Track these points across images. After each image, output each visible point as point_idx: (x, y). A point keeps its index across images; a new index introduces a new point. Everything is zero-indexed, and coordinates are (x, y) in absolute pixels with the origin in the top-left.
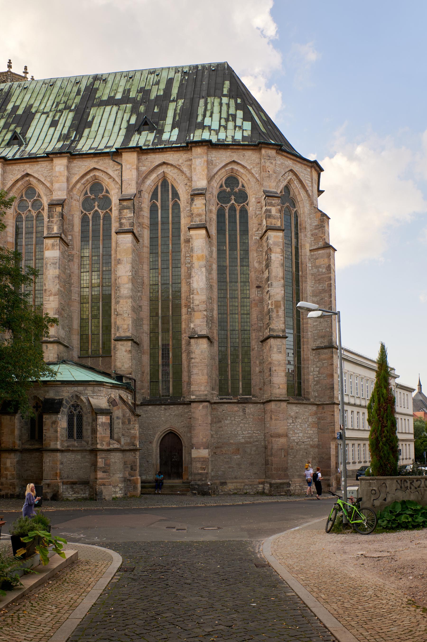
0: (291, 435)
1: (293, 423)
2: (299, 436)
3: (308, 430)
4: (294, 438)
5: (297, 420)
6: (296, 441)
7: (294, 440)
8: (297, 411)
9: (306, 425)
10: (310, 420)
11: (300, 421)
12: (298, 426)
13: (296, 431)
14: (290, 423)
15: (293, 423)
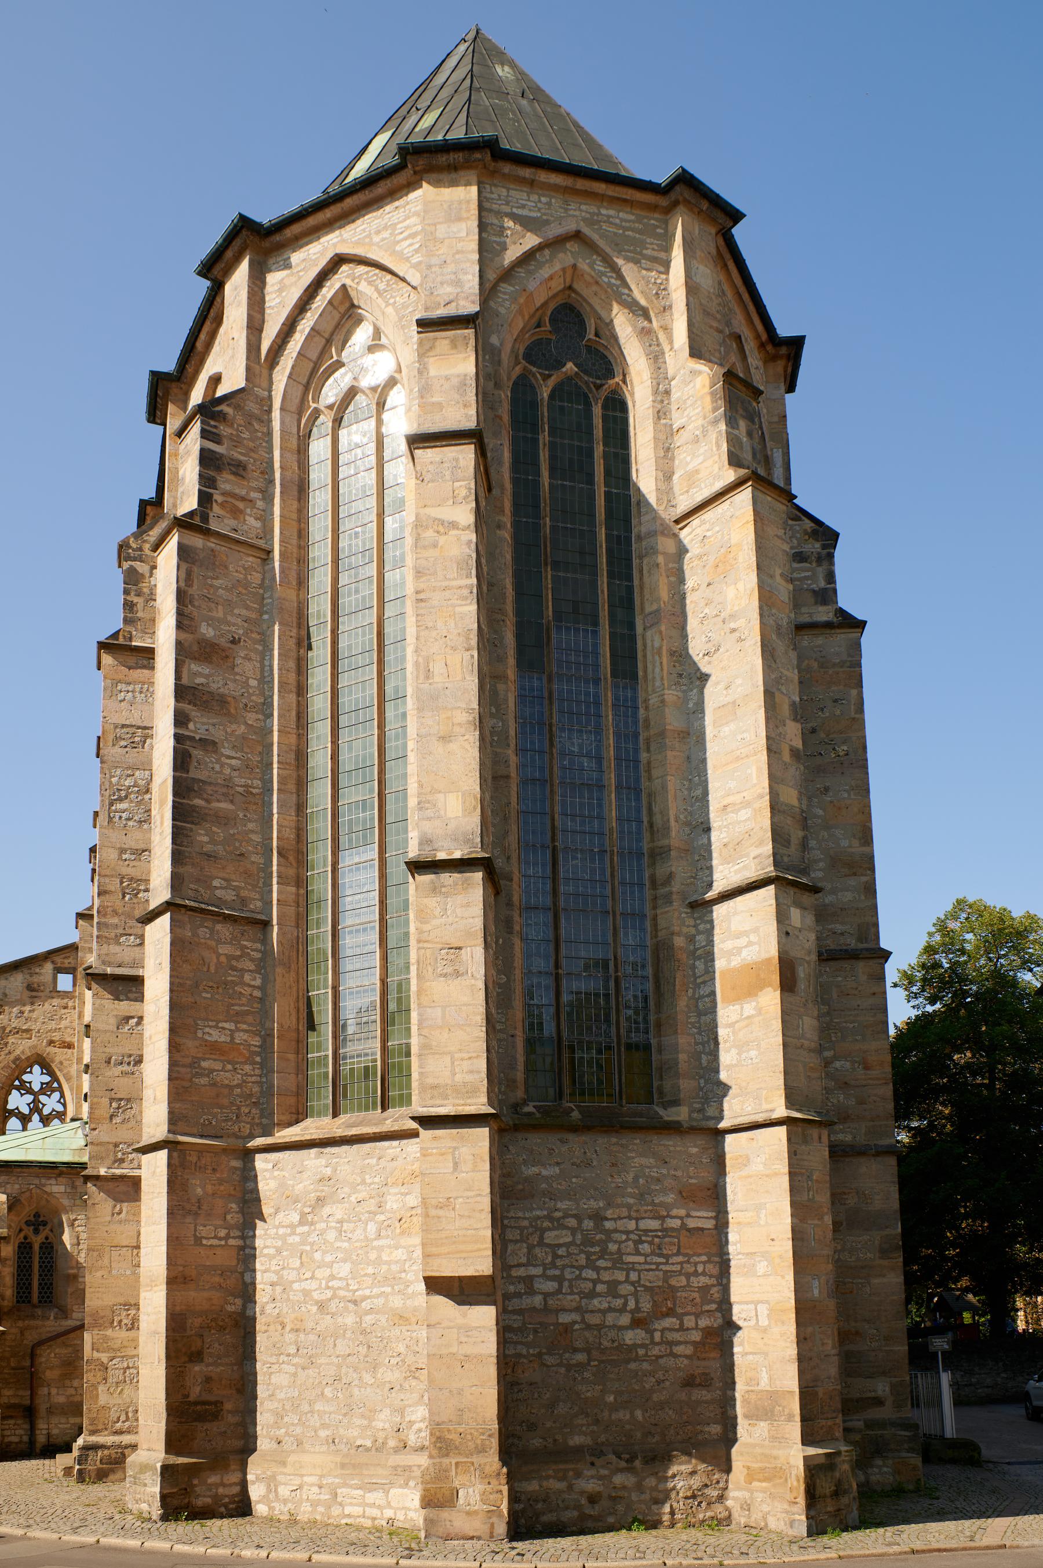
0: (292, 1276)
1: (301, 1223)
2: (332, 1277)
3: (380, 1249)
4: (307, 1285)
5: (327, 1210)
6: (316, 1295)
7: (306, 1293)
8: (328, 1171)
9: (372, 1228)
10: (392, 1203)
11: (338, 1211)
12: (331, 1236)
13: (317, 1256)
14: (292, 1226)
15: (301, 1223)
